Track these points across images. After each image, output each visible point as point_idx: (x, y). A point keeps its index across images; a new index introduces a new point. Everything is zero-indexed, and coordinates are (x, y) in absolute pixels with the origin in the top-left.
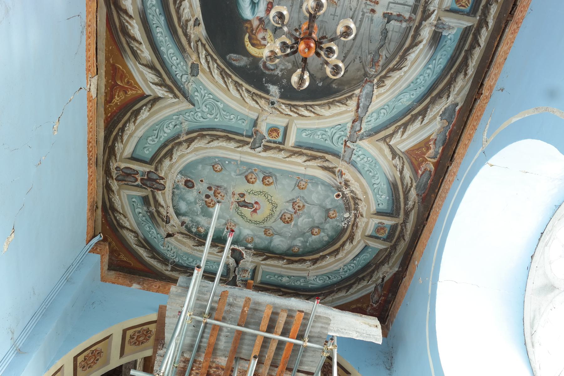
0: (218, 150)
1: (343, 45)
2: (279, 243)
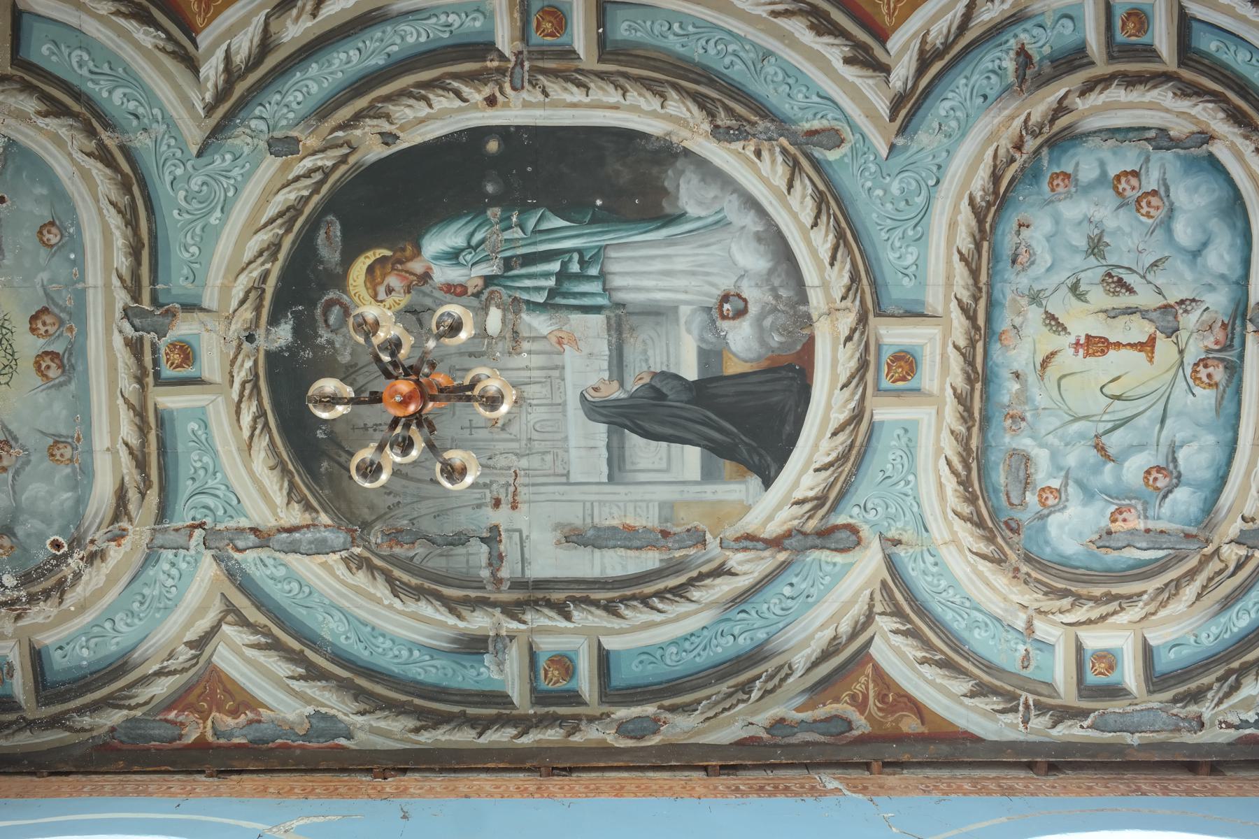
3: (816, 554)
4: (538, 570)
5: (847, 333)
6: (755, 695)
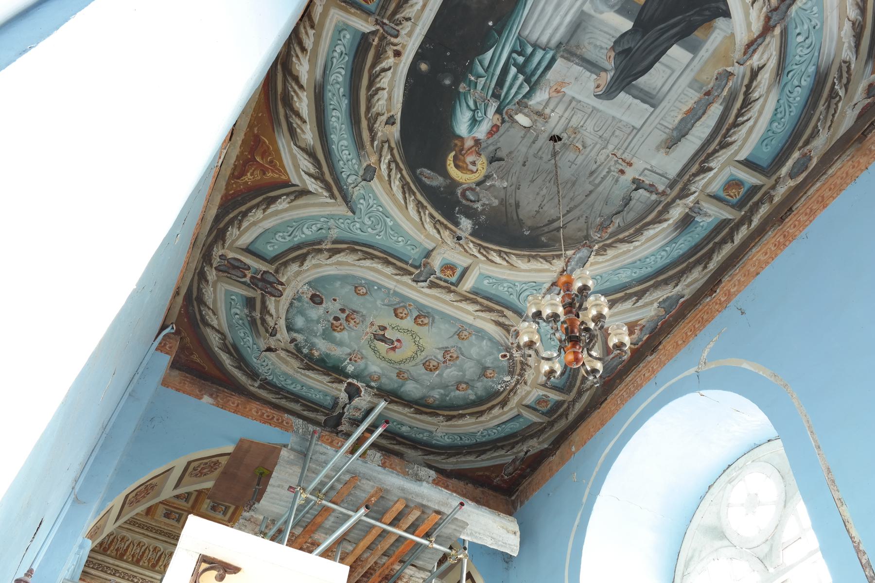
0: (369, 272)
1: (571, 199)
2: (411, 389)
4: (673, 172)
6: (841, 93)
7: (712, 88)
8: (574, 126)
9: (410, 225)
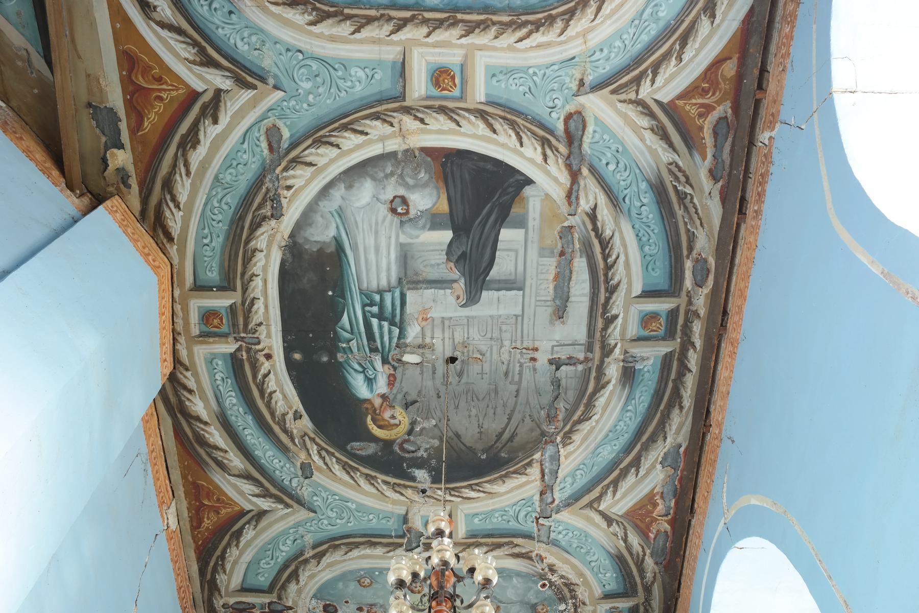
1: (503, 406)
3: (585, 146)
5: (418, 123)
6: (688, 190)
7: (563, 247)
8: (461, 341)
9: (372, 500)
